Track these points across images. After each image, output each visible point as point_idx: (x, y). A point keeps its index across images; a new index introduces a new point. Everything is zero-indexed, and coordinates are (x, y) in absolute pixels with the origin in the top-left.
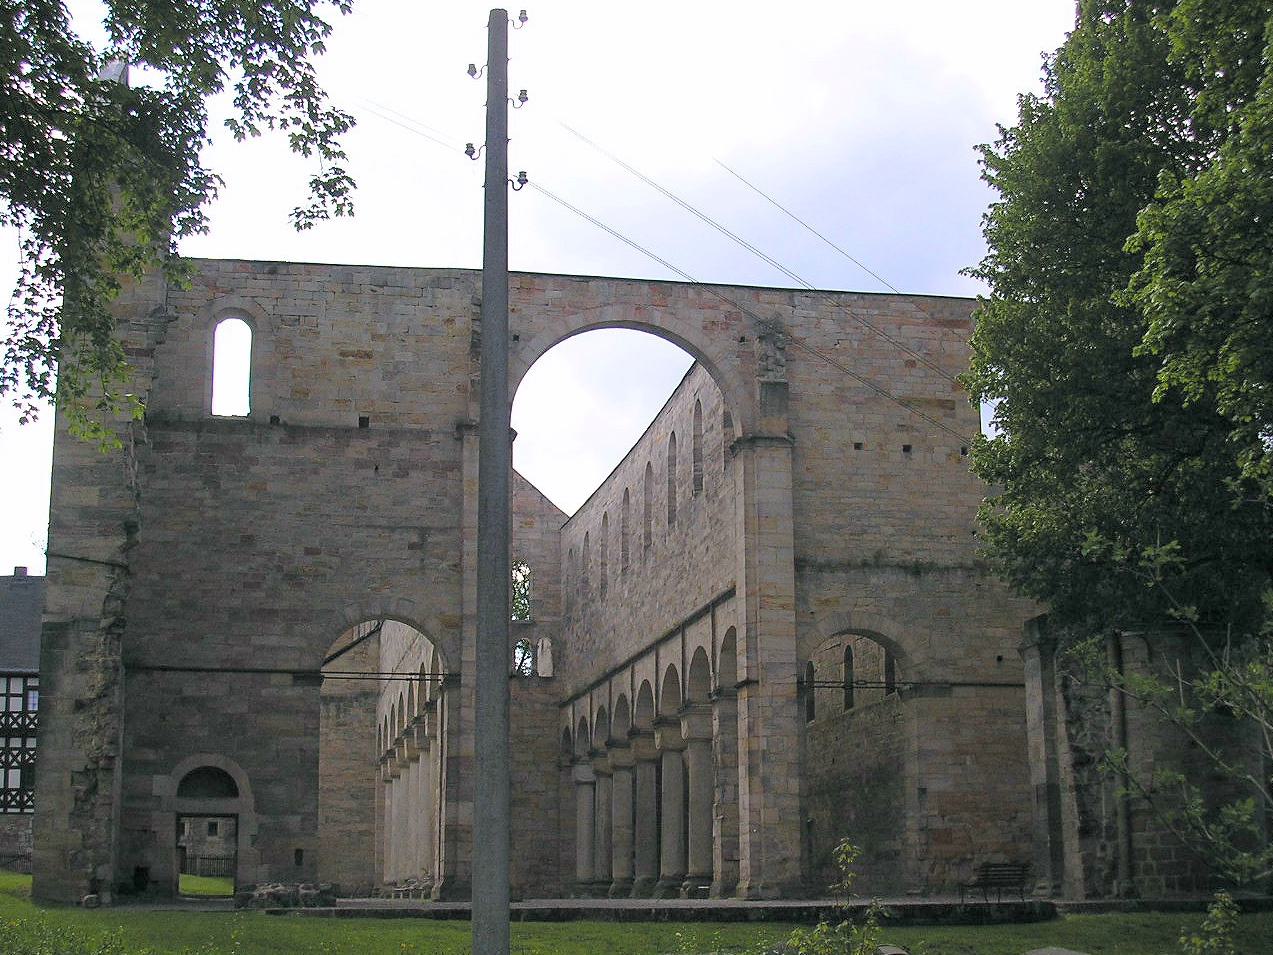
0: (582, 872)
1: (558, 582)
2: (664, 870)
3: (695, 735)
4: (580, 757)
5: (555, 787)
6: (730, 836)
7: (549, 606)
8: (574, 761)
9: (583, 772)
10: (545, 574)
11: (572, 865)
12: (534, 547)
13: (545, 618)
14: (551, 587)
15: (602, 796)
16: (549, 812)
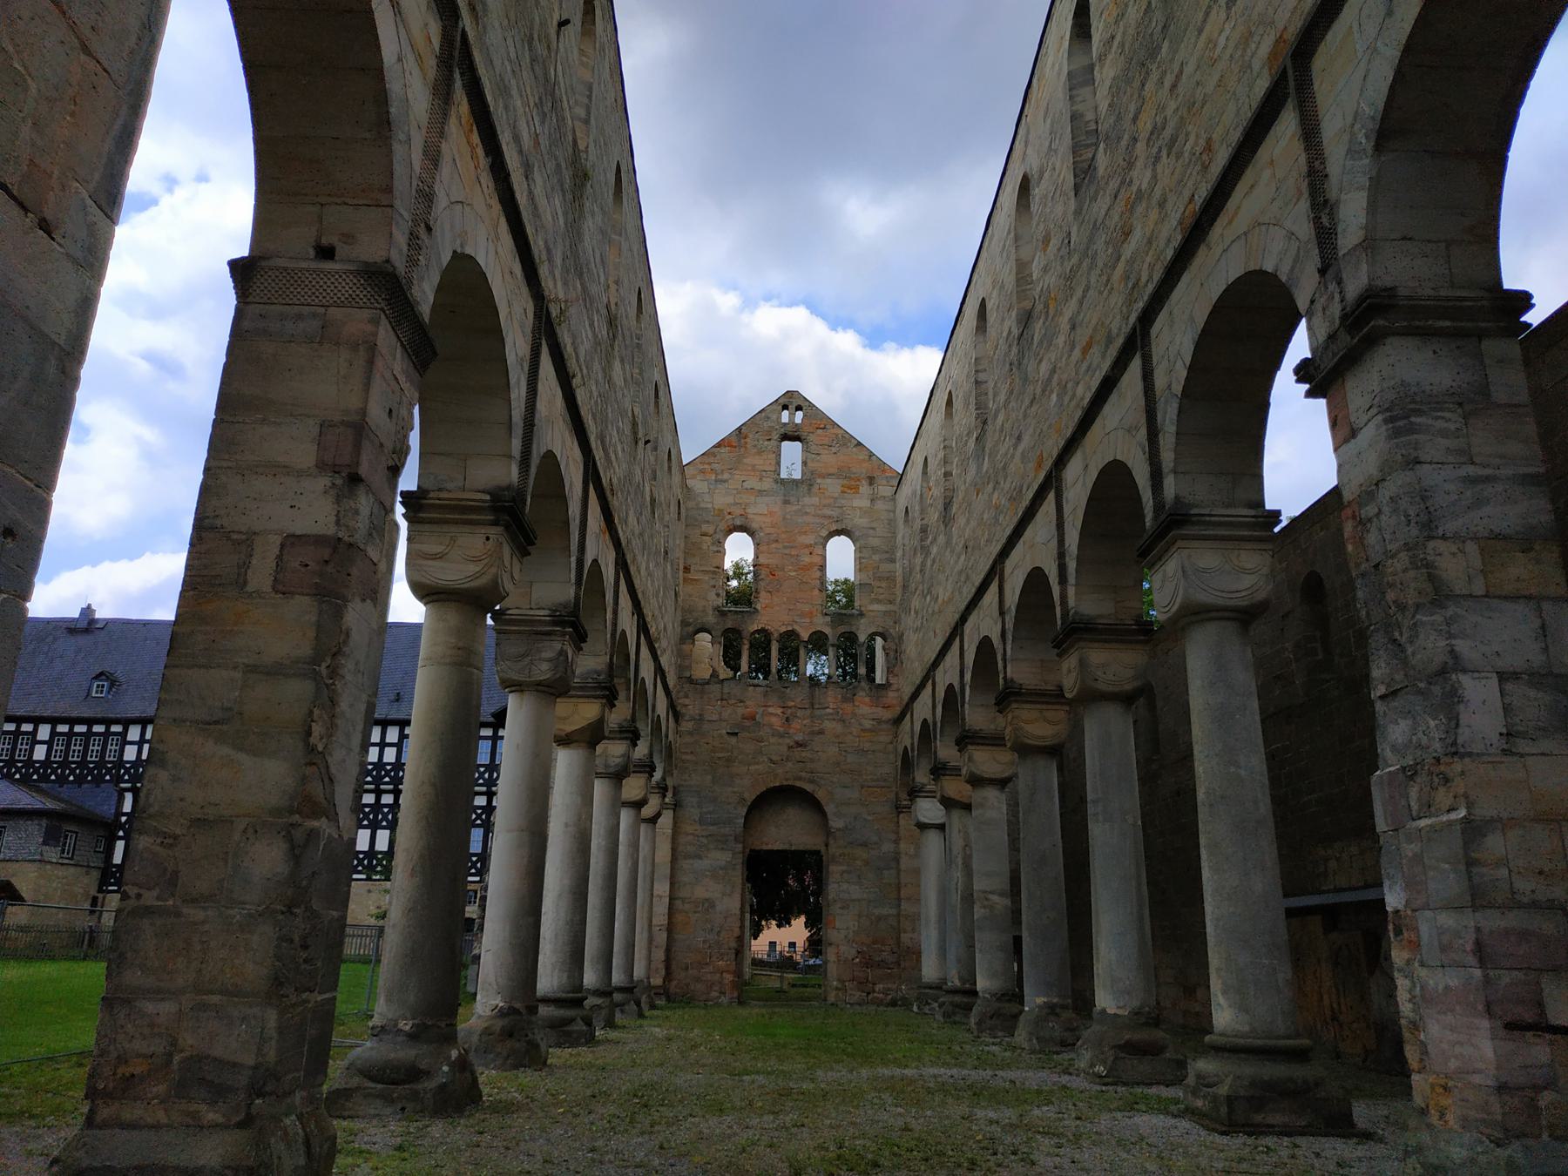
0: (930, 970)
1: (893, 561)
2: (1105, 1000)
3: (1203, 597)
4: (924, 785)
5: (893, 837)
6: (1514, 903)
7: (881, 591)
8: (914, 793)
9: (929, 810)
10: (875, 550)
11: (914, 954)
12: (860, 517)
13: (876, 607)
14: (885, 567)
15: (957, 842)
16: (886, 872)
